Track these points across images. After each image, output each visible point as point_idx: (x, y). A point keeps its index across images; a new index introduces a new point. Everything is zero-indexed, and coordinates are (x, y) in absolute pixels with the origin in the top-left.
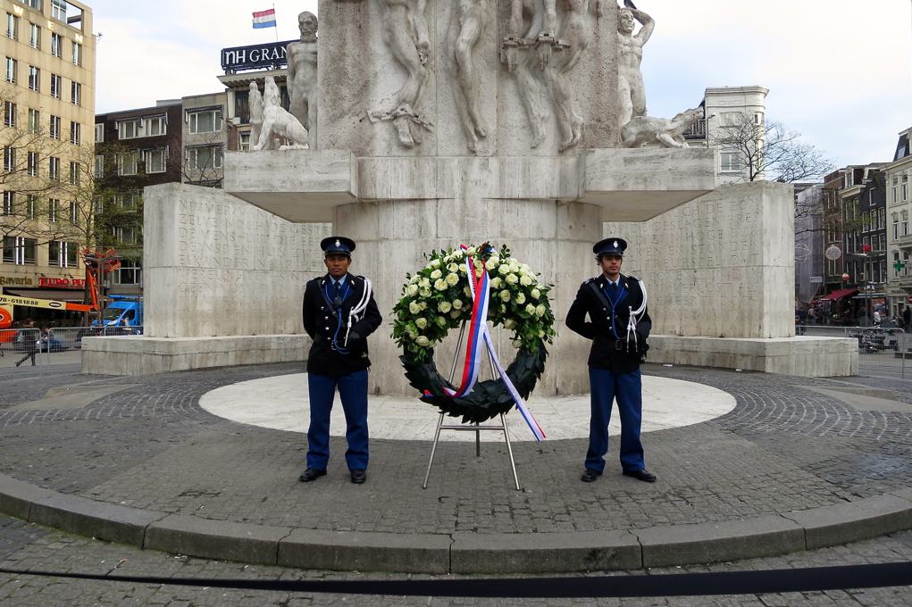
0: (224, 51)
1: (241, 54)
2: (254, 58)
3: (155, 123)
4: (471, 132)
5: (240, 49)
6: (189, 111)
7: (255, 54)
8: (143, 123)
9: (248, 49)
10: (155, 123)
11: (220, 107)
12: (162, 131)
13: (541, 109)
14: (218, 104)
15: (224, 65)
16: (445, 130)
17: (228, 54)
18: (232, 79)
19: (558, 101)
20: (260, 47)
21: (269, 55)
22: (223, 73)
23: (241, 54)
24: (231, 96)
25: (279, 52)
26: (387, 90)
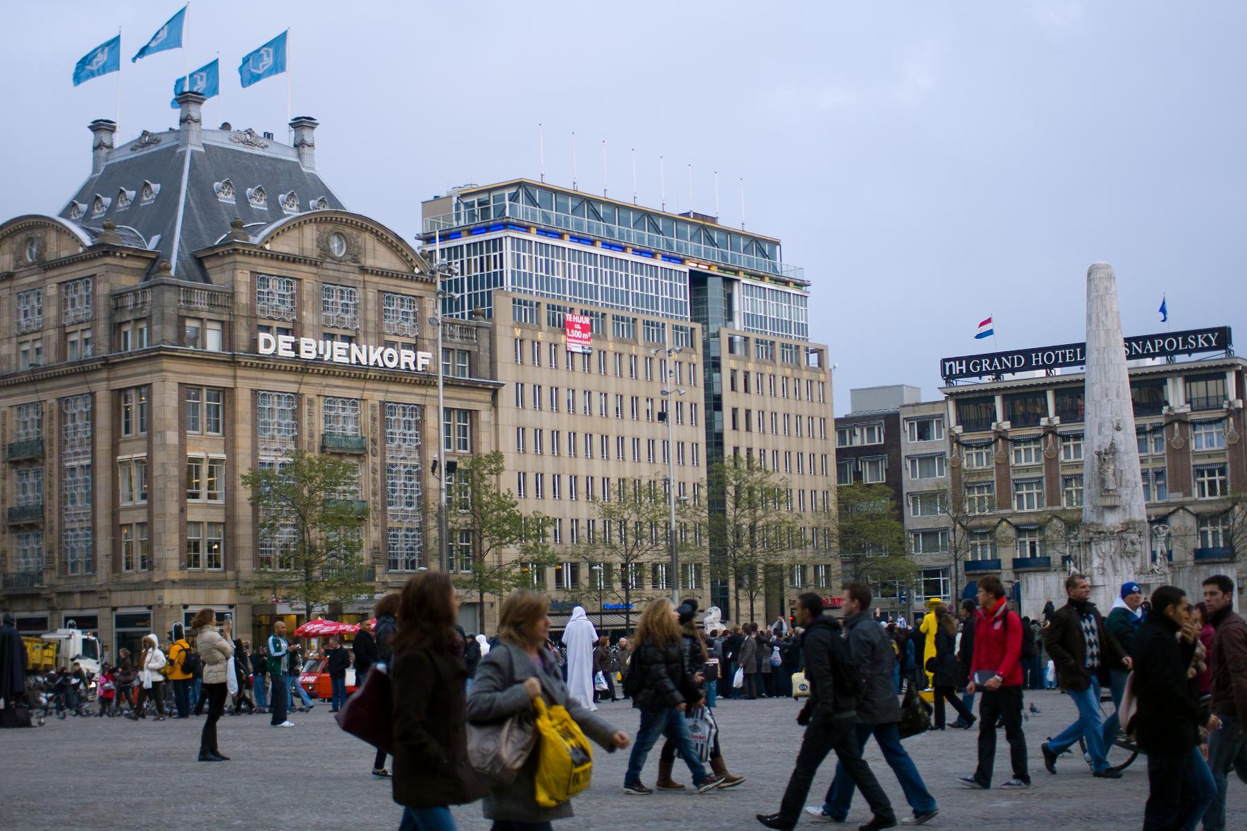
0: (945, 360)
1: (961, 365)
2: (975, 368)
3: (871, 430)
4: (1115, 570)
5: (960, 359)
6: (906, 419)
7: (975, 364)
8: (858, 431)
9: (969, 359)
10: (871, 430)
11: (942, 416)
12: (879, 440)
13: (1130, 565)
14: (937, 412)
15: (943, 374)
16: (1109, 570)
17: (947, 365)
18: (949, 391)
19: (1134, 563)
20: (980, 357)
21: (990, 365)
22: (943, 383)
23: (961, 365)
24: (951, 405)
25: (1000, 362)
26: (1096, 562)
